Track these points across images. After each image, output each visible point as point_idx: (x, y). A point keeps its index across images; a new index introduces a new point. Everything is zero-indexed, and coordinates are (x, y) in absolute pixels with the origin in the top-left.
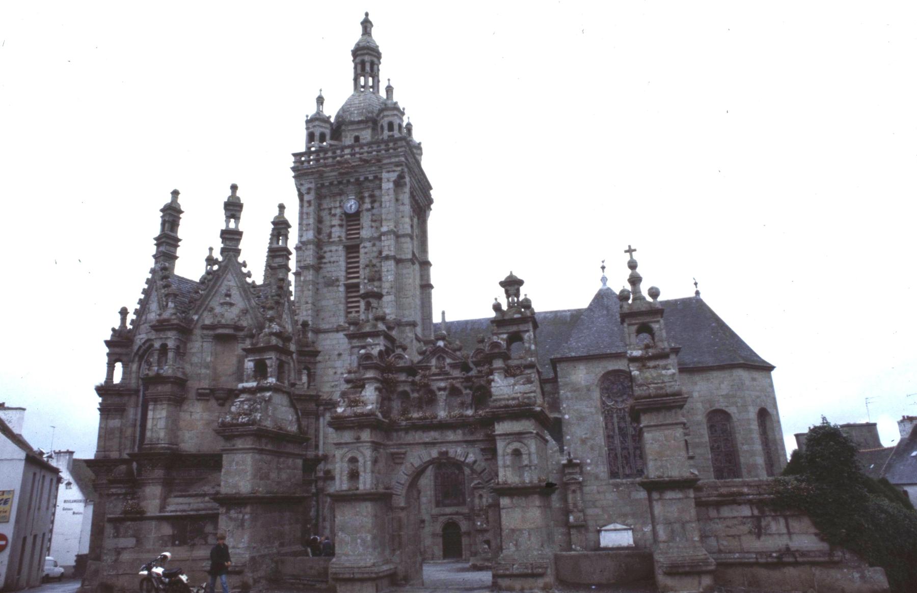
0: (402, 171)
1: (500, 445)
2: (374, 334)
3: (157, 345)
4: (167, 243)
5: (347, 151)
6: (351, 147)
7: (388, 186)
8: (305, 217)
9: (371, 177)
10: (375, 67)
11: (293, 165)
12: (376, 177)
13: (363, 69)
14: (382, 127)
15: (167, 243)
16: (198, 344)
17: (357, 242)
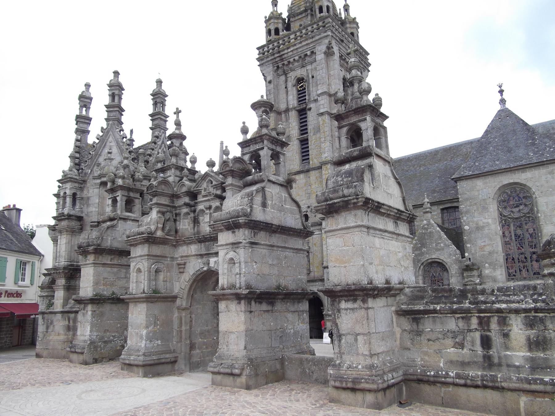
4: (83, 121)
7: (320, 57)
9: (309, 53)
11: (258, 56)
12: (312, 53)
15: (83, 121)
16: (91, 191)
17: (305, 106)
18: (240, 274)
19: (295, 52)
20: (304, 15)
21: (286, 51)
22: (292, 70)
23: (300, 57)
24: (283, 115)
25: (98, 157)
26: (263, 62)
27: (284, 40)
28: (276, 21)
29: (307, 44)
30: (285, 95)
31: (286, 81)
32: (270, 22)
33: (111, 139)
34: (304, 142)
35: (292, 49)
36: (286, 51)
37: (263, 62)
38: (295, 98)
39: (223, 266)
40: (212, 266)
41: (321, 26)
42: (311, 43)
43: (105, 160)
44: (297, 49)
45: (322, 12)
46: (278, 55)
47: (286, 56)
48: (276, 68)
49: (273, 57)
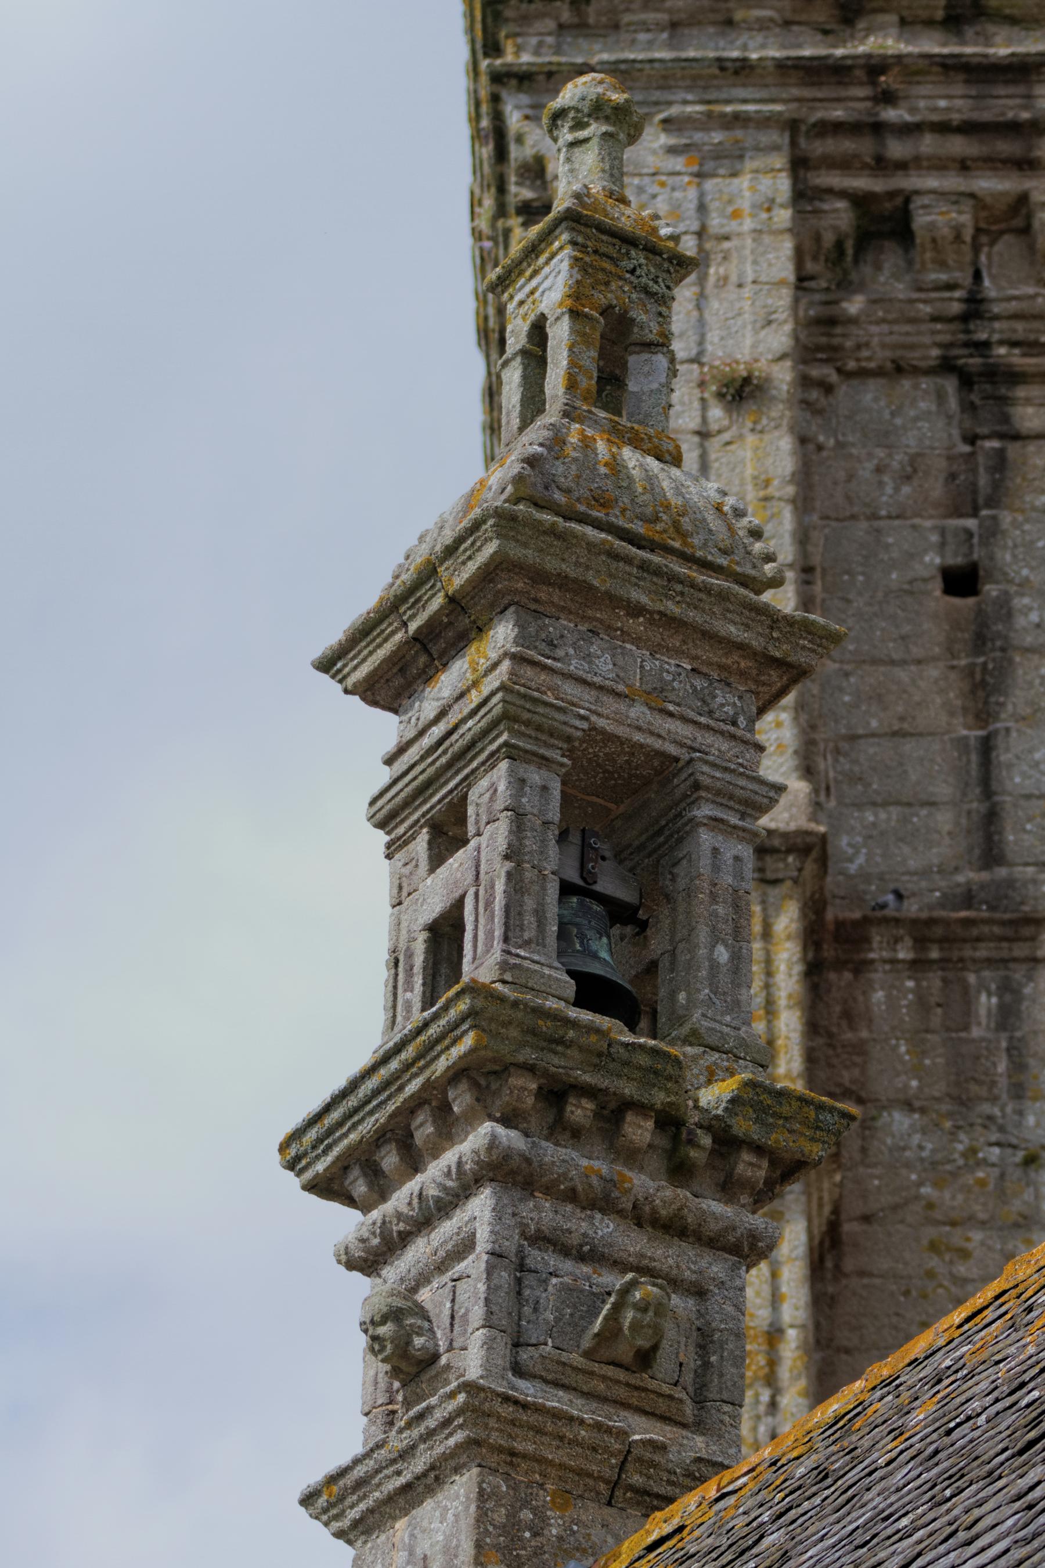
48: (840, 216)
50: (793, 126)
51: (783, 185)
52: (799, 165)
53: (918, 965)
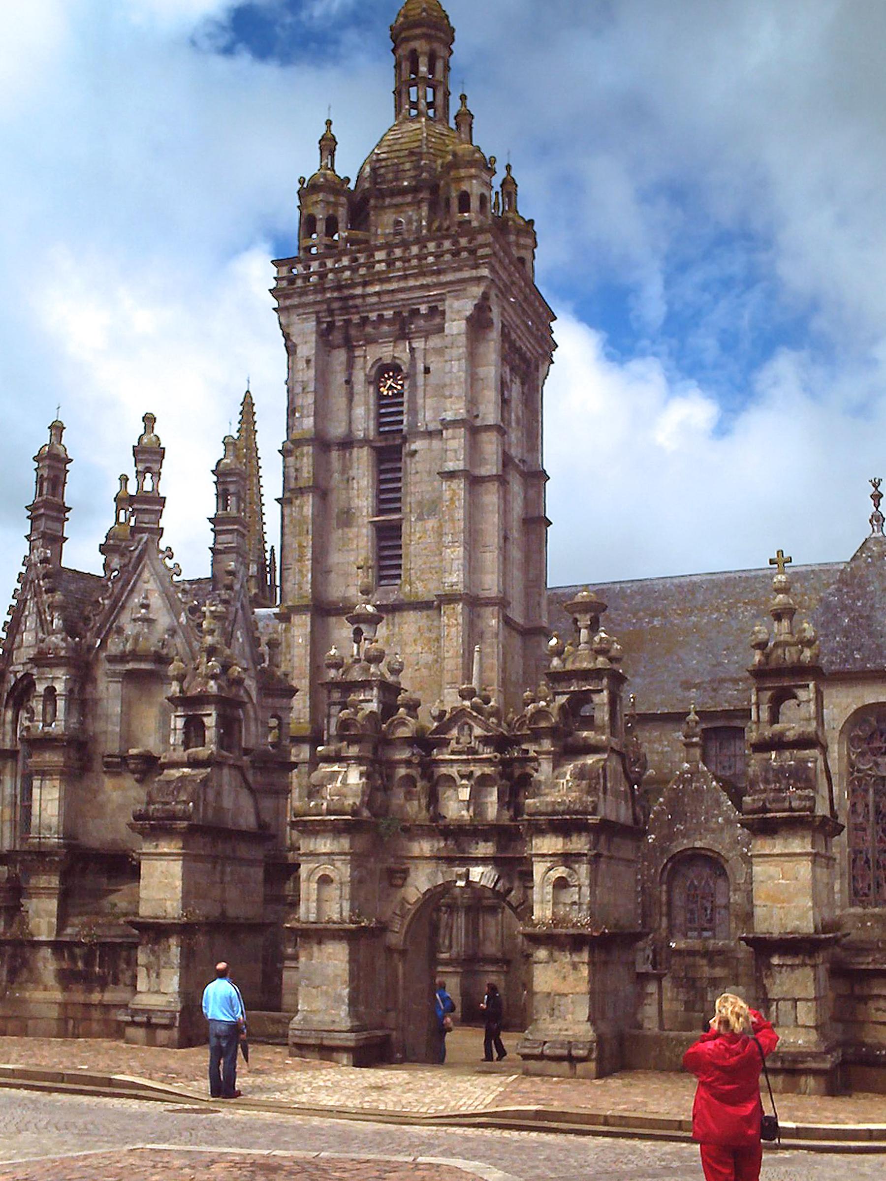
0: (485, 297)
1: (539, 869)
2: (366, 685)
3: (40, 688)
5: (380, 255)
6: (388, 247)
7: (456, 327)
8: (298, 389)
9: (423, 309)
10: (439, 65)
11: (273, 284)
12: (434, 311)
13: (415, 70)
14: (448, 201)
17: (398, 441)
18: (581, 904)
19: (386, 298)
20: (409, 198)
21: (358, 291)
22: (370, 341)
23: (398, 314)
24: (335, 454)
25: (119, 613)
26: (288, 302)
27: (355, 260)
28: (332, 199)
29: (422, 287)
30: (342, 402)
31: (350, 365)
32: (314, 198)
33: (146, 575)
34: (388, 536)
35: (377, 288)
36: (358, 291)
37: (288, 302)
38: (372, 415)
39: (543, 888)
40: (477, 879)
41: (465, 249)
42: (436, 285)
43: (135, 620)
44: (393, 291)
45: (468, 211)
46: (335, 295)
47: (359, 301)
48: (325, 325)
49: (319, 298)
50: (317, 313)
51: (314, 323)
52: (317, 317)
53: (338, 450)
